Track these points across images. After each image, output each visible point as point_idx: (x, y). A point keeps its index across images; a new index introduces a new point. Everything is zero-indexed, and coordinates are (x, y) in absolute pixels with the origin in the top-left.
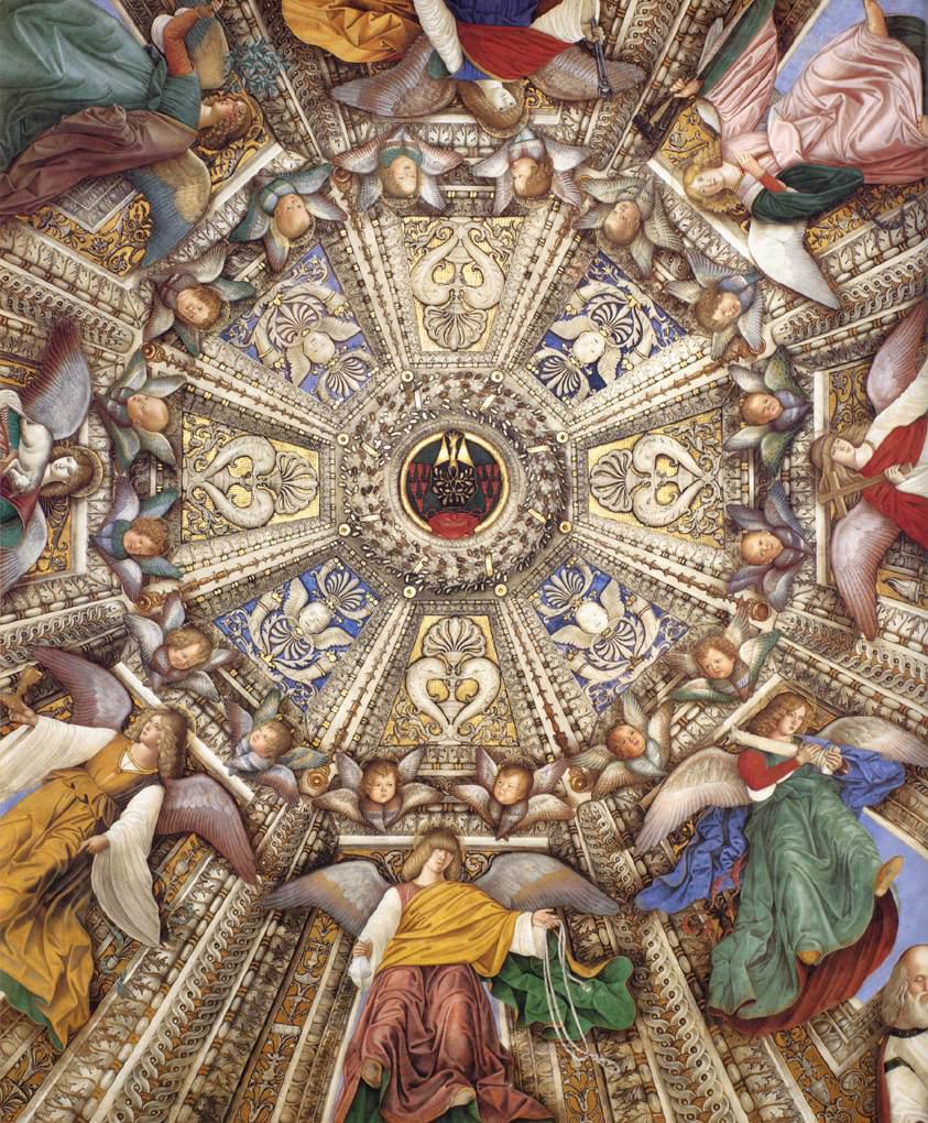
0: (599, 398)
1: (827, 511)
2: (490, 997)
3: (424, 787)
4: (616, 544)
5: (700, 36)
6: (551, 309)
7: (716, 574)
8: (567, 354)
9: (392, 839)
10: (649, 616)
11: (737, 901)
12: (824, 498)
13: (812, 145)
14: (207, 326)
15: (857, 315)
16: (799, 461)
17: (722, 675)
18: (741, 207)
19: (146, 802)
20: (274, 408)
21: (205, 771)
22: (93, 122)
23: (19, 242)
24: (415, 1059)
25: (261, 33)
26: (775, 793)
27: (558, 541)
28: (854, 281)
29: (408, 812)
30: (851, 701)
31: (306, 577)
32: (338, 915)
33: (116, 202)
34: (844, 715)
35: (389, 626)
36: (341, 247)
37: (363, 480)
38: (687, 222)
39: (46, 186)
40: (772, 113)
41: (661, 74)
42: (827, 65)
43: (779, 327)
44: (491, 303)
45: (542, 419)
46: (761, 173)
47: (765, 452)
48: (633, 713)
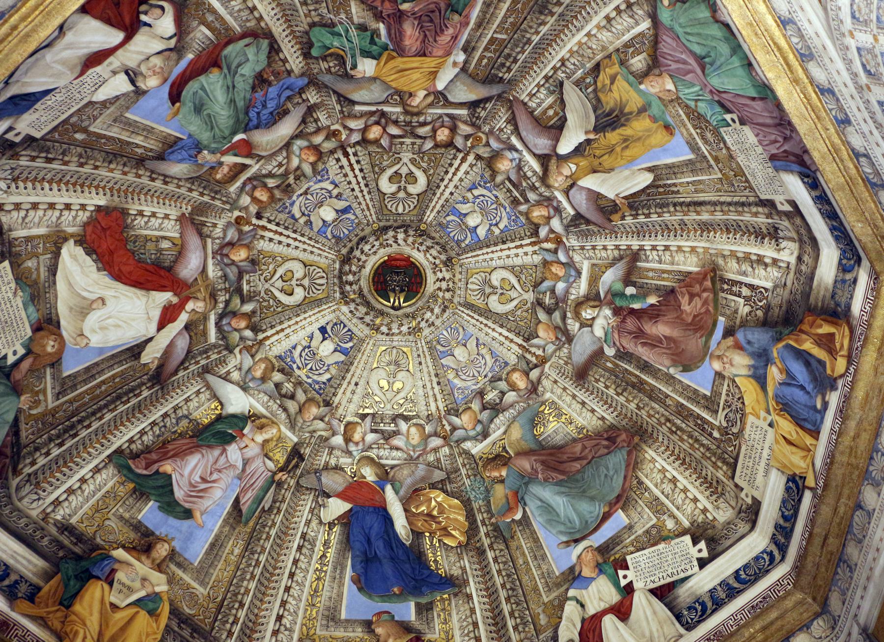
0: (322, 322)
1: (207, 276)
2: (389, 43)
3: (420, 134)
4: (315, 250)
5: (274, 501)
6: (346, 367)
7: (262, 237)
8: (338, 345)
9: (440, 111)
10: (298, 215)
11: (254, 89)
12: (209, 282)
13: (221, 454)
14: (514, 370)
15: (196, 372)
16: (222, 299)
17: (259, 189)
18: (253, 421)
19: (565, 147)
20: (486, 325)
21: (535, 155)
22: (554, 475)
23: (594, 422)
24: (431, 21)
25: (475, 506)
26: (232, 138)
27: (344, 251)
28: (198, 388)
29: (429, 123)
30: (193, 184)
31: (477, 239)
32: (469, 80)
33: (549, 436)
34: (197, 177)
35: (435, 210)
36: (447, 402)
37: (444, 285)
38: (278, 412)
39: (578, 448)
40: (241, 468)
41: (292, 482)
42: (217, 493)
43: (233, 361)
44: (375, 371)
45: (351, 312)
46: (244, 439)
47: (238, 301)
48: (307, 169)
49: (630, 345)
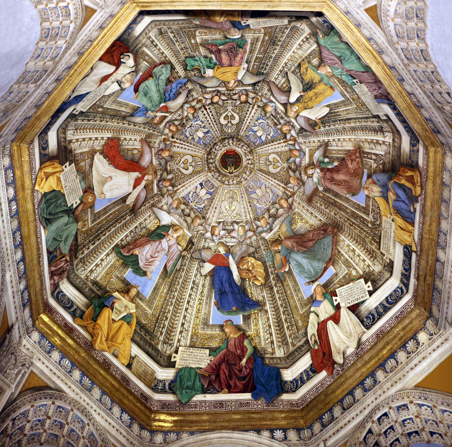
49: (329, 185)
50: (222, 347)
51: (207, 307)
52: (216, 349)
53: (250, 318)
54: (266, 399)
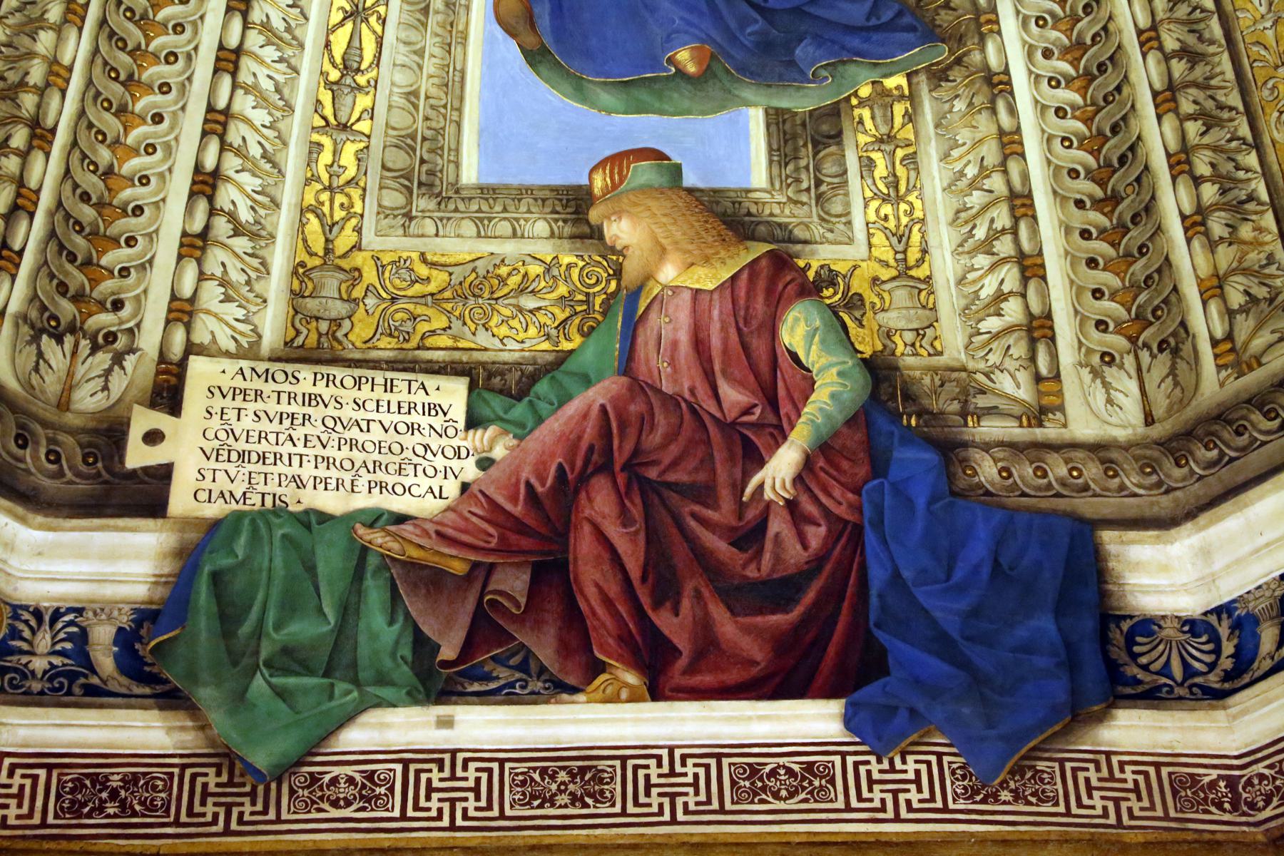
50: (588, 358)
51: (431, 45)
52: (534, 378)
53: (837, 137)
54: (965, 743)
